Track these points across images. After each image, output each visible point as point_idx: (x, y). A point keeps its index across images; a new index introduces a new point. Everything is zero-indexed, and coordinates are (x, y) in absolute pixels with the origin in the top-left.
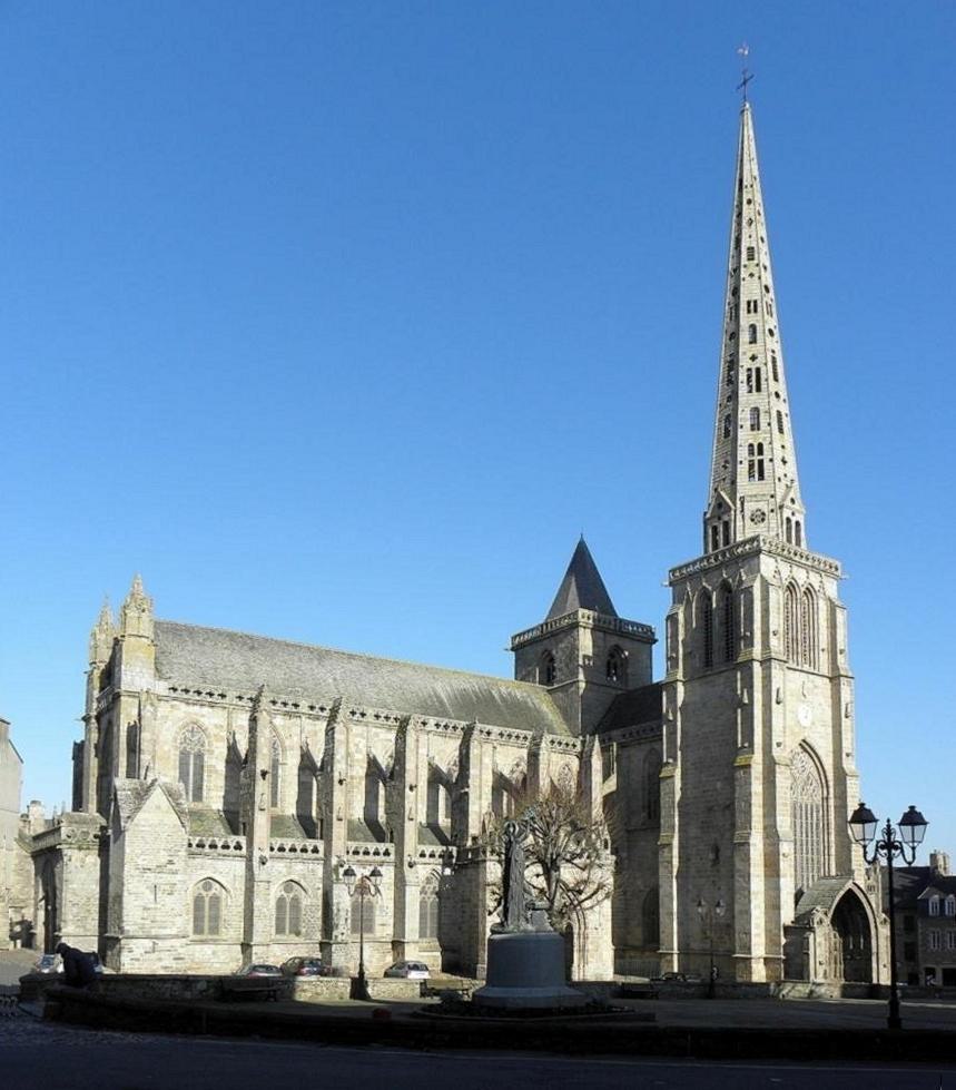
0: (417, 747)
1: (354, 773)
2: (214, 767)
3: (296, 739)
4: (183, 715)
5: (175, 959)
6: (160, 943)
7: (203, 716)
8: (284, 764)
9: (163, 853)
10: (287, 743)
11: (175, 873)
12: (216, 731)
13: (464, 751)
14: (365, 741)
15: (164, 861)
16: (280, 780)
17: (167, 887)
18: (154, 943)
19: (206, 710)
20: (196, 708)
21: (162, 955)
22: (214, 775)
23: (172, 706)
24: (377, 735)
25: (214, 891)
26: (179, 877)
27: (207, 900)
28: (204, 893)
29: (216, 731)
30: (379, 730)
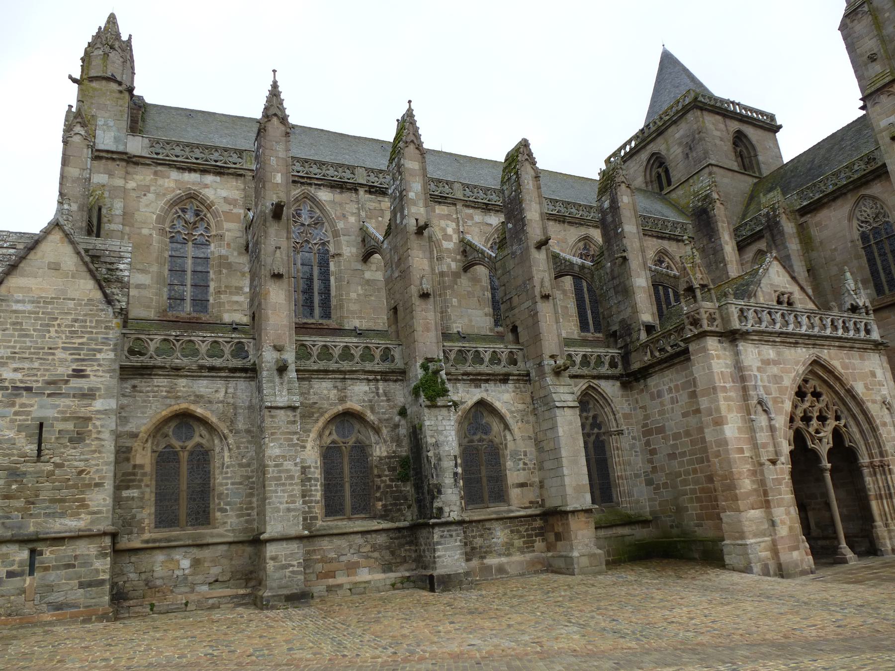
0: (539, 188)
1: (445, 269)
2: (227, 258)
3: (352, 219)
4: (172, 185)
5: (81, 585)
6: (49, 554)
7: (206, 186)
8: (339, 255)
9: (60, 354)
10: (340, 225)
11: (89, 395)
12: (226, 207)
13: (606, 204)
14: (454, 225)
15: (64, 371)
16: (332, 279)
17: (70, 426)
18: (33, 552)
19: (209, 179)
20: (194, 177)
21: (52, 577)
22: (224, 271)
23: (156, 173)
24: (472, 218)
25: (197, 439)
26: (99, 404)
27: (184, 456)
28: (177, 444)
29: (226, 207)
30: (471, 211)
